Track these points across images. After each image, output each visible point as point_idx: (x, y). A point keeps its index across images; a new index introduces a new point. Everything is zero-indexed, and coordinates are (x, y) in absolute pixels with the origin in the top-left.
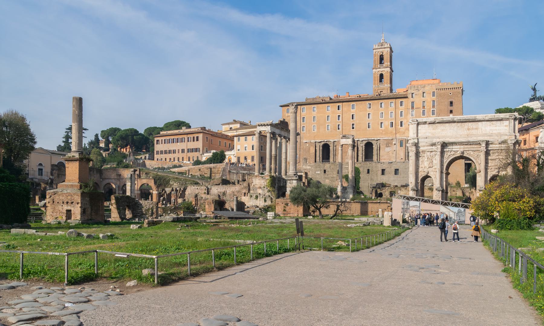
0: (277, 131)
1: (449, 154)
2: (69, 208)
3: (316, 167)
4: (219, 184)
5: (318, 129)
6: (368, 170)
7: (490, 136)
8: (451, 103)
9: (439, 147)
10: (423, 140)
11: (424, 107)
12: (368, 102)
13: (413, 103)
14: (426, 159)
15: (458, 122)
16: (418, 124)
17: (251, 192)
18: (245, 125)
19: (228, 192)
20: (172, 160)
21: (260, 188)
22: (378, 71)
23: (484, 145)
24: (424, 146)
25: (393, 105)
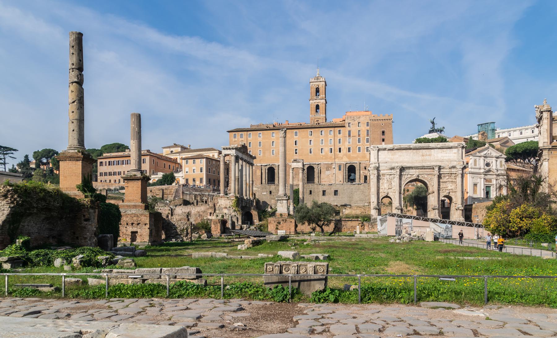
0: (240, 155)
1: (406, 177)
2: (135, 229)
3: (263, 189)
4: (180, 205)
5: (264, 153)
6: (311, 191)
7: (441, 161)
8: (383, 132)
9: (398, 170)
10: (383, 164)
11: (359, 135)
12: (309, 130)
13: (349, 131)
14: (386, 182)
15: (414, 149)
16: (379, 150)
17: (217, 212)
18: (185, 148)
19: (193, 212)
20: (117, 182)
21: (226, 208)
22: (314, 102)
23: (437, 169)
24: (384, 170)
25: (332, 133)
